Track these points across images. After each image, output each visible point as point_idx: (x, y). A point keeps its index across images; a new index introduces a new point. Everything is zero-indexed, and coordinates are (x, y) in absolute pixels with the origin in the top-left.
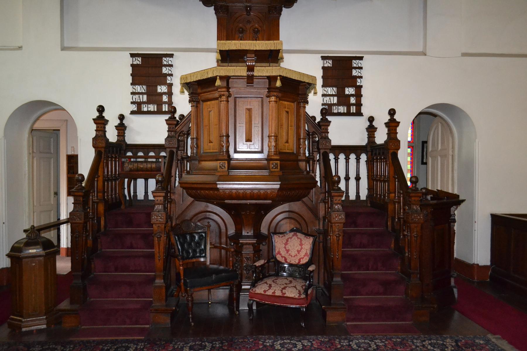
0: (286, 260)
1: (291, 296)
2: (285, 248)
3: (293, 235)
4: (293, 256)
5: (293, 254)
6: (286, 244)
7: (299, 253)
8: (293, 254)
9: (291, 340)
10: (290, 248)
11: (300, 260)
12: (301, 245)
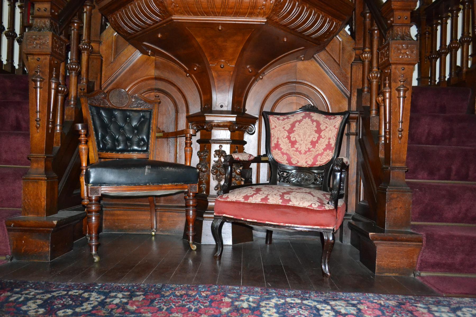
1: (302, 205)
2: (289, 138)
3: (304, 117)
6: (291, 131)
7: (314, 147)
8: (303, 149)
9: (302, 299)
10: (298, 139)
12: (319, 131)
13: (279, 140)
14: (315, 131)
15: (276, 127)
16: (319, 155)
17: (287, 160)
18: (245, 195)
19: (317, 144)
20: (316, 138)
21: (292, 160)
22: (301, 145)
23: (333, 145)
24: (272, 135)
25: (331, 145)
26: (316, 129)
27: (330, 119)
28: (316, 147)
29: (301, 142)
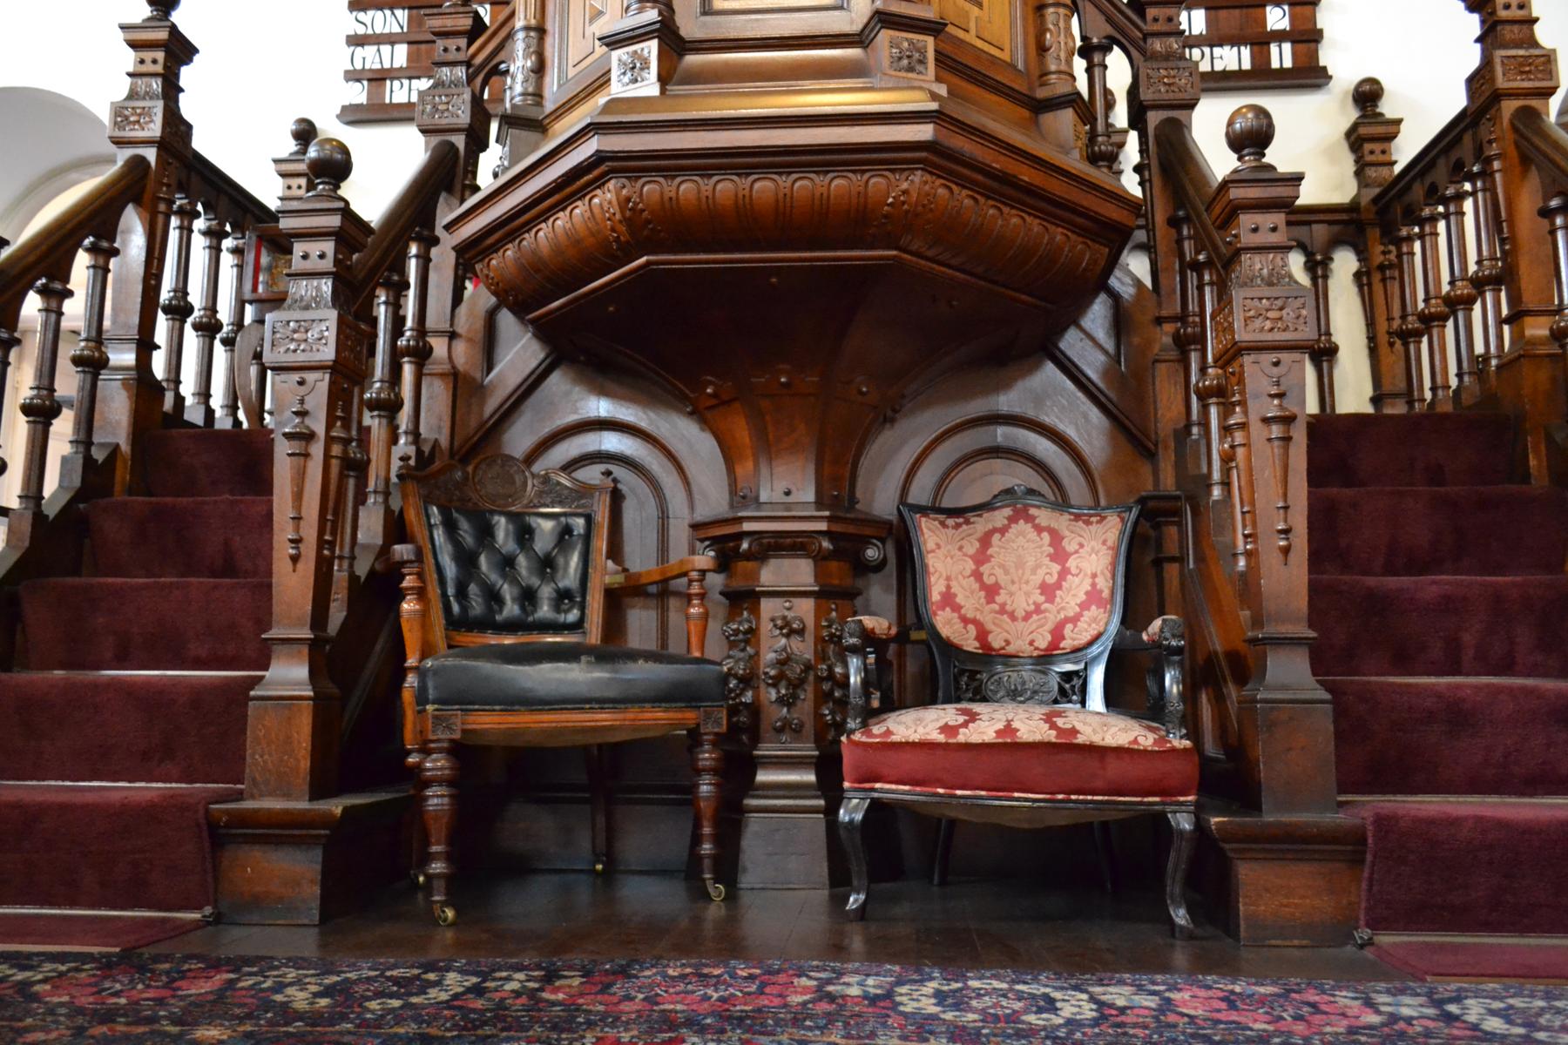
0: (982, 635)
2: (977, 575)
3: (1013, 520)
4: (1020, 613)
5: (1021, 605)
6: (981, 558)
8: (1021, 605)
10: (1003, 579)
11: (1057, 634)
12: (1060, 556)
13: (953, 583)
14: (1049, 555)
15: (938, 546)
16: (1066, 620)
17: (977, 638)
18: (941, 723)
19: (1058, 593)
20: (1056, 576)
21: (990, 638)
22: (1011, 594)
23: (1106, 594)
24: (931, 570)
25: (1101, 591)
26: (1051, 550)
27: (1088, 523)
28: (1058, 600)
29: (1013, 588)
